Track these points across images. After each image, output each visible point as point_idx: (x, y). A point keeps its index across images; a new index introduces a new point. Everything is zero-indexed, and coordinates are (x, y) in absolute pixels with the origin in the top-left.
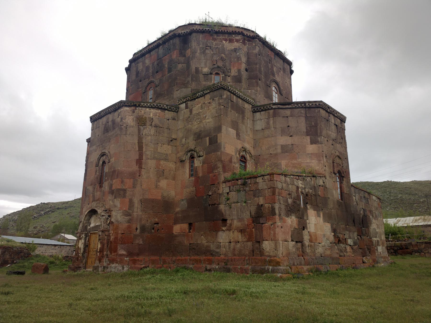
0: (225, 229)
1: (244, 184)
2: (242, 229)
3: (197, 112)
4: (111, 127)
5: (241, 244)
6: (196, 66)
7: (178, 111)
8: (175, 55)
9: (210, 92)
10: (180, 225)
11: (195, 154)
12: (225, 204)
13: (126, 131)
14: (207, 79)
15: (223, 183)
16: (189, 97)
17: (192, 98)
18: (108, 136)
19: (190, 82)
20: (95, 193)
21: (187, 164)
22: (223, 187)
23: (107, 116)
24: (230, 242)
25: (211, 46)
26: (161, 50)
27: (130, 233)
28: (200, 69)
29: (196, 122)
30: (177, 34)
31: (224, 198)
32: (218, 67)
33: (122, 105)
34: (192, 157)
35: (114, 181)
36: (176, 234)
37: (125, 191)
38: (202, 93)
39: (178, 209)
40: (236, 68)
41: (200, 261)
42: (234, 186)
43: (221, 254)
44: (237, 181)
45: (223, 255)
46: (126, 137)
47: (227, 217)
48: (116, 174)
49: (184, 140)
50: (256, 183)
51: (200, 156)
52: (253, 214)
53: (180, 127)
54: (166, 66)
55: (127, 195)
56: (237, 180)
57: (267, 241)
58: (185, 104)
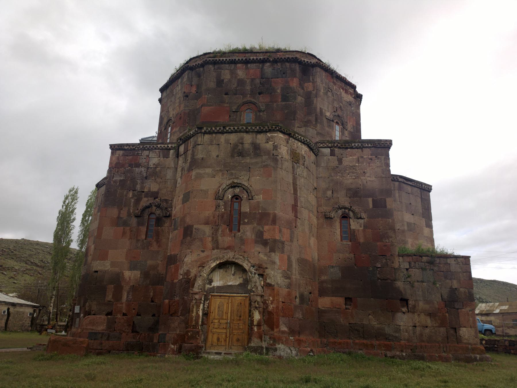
0: (406, 311)
1: (431, 263)
2: (431, 312)
3: (351, 165)
4: (251, 152)
5: (430, 329)
6: (321, 107)
7: (318, 155)
8: (294, 83)
9: (372, 147)
10: (330, 298)
11: (351, 214)
12: (404, 282)
13: (282, 164)
14: (330, 126)
15: (399, 256)
16: (339, 143)
17: (343, 146)
18: (243, 162)
19: (314, 123)
20: (220, 238)
21: (337, 223)
22: (400, 261)
23: (238, 134)
24: (415, 327)
25: (332, 89)
27: (290, 302)
28: (324, 111)
29: (349, 176)
30: (299, 60)
31: (402, 274)
32: (338, 116)
33: (277, 129)
34: (345, 217)
35: (266, 228)
36: (323, 309)
37: (283, 243)
38: (360, 144)
39: (324, 278)
40: (351, 123)
41: (373, 346)
42: (417, 263)
43: (401, 340)
44: (420, 258)
45: (404, 340)
46: (282, 172)
47: (408, 296)
48: (271, 219)
49: (329, 193)
50: (447, 264)
51: (361, 218)
52: (445, 296)
53: (321, 175)
54: (279, 91)
55: (285, 249)
56: (421, 256)
57: (465, 328)
58: (329, 149)
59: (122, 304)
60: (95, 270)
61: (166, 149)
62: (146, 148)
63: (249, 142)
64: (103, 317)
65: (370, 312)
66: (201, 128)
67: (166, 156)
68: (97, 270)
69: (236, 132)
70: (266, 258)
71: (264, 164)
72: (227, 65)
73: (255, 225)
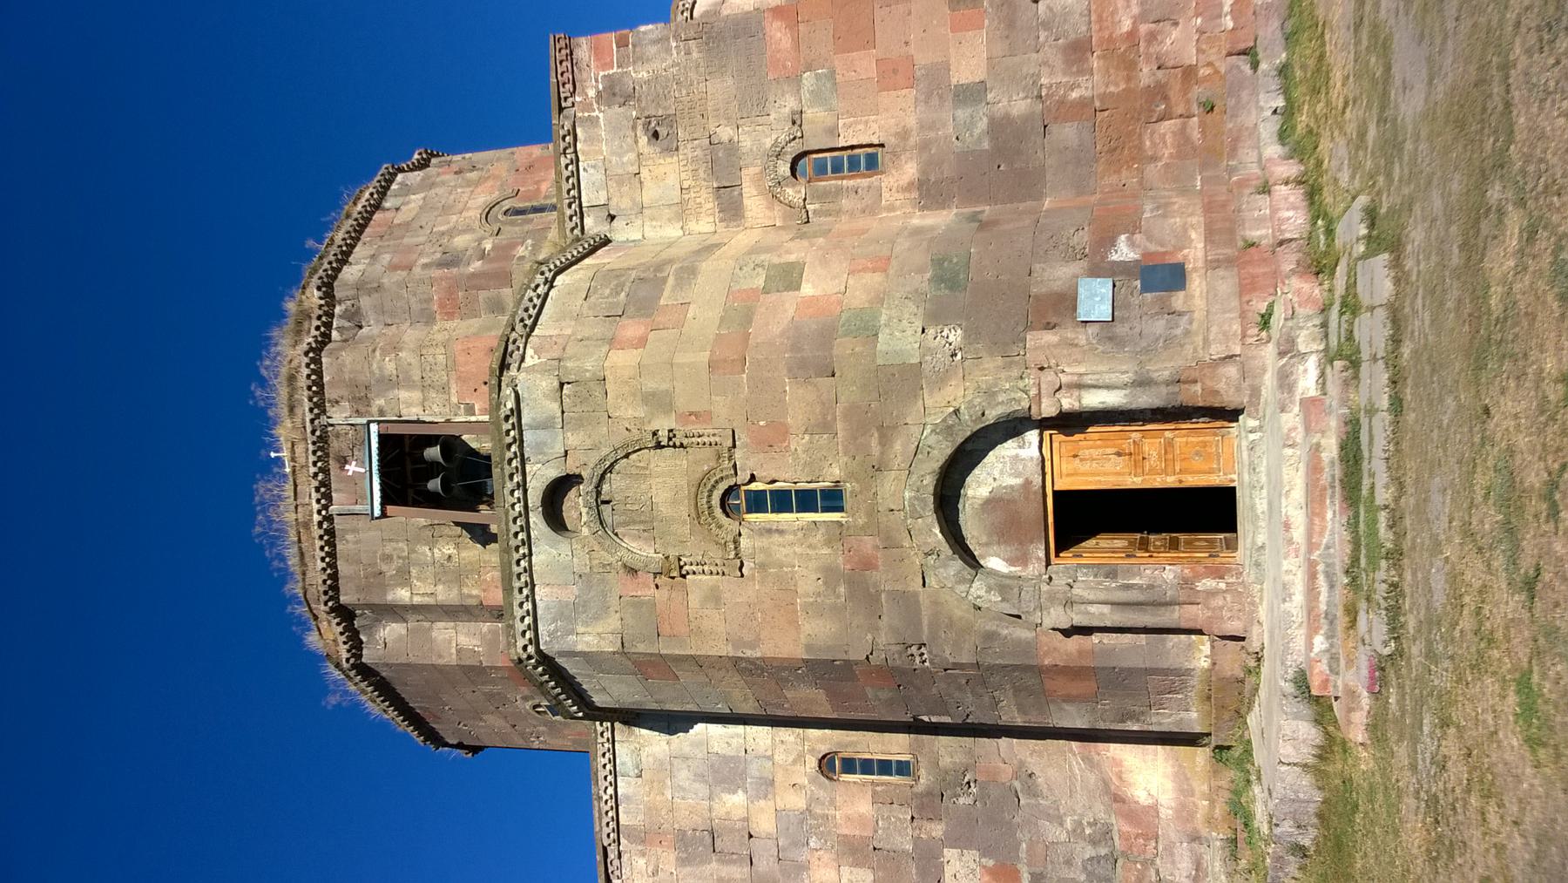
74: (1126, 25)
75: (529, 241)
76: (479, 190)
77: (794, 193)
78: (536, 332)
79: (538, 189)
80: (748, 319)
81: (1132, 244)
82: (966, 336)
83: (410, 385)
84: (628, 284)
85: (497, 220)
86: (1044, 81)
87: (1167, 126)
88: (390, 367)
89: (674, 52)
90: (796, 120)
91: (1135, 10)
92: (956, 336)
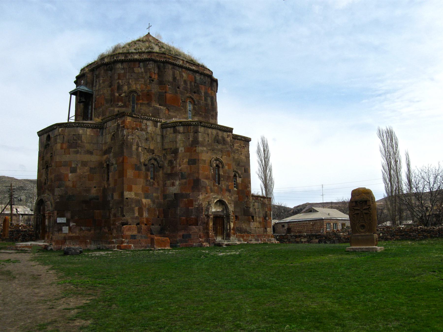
11: (237, 175)
26: (198, 77)
51: (241, 177)
54: (203, 94)
59: (144, 218)
60: (127, 197)
61: (156, 121)
62: (145, 119)
63: (221, 135)
64: (135, 226)
65: (243, 222)
66: (201, 123)
67: (156, 126)
68: (128, 197)
69: (216, 129)
70: (230, 199)
71: (227, 149)
72: (178, 68)
73: (225, 182)
74: (117, 223)
75: (123, 104)
76: (142, 85)
77: (105, 165)
78: (66, 128)
79: (140, 100)
80: (64, 166)
81: (73, 225)
82: (58, 201)
83: (99, 88)
84: (76, 142)
85: (131, 94)
86: (113, 210)
87: (107, 231)
88: (101, 81)
89: (121, 138)
90: (113, 164)
91: (118, 225)
92: (58, 200)
